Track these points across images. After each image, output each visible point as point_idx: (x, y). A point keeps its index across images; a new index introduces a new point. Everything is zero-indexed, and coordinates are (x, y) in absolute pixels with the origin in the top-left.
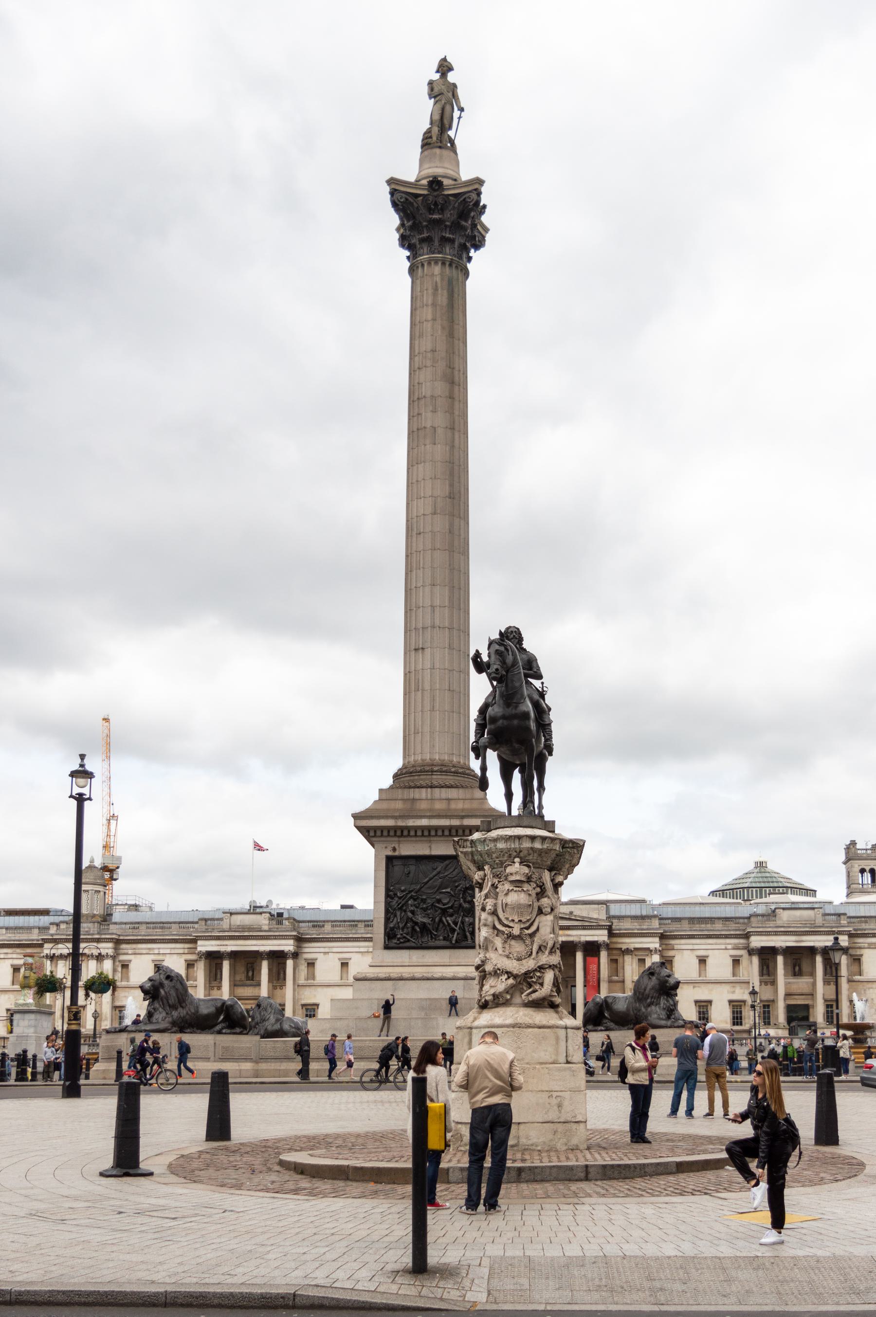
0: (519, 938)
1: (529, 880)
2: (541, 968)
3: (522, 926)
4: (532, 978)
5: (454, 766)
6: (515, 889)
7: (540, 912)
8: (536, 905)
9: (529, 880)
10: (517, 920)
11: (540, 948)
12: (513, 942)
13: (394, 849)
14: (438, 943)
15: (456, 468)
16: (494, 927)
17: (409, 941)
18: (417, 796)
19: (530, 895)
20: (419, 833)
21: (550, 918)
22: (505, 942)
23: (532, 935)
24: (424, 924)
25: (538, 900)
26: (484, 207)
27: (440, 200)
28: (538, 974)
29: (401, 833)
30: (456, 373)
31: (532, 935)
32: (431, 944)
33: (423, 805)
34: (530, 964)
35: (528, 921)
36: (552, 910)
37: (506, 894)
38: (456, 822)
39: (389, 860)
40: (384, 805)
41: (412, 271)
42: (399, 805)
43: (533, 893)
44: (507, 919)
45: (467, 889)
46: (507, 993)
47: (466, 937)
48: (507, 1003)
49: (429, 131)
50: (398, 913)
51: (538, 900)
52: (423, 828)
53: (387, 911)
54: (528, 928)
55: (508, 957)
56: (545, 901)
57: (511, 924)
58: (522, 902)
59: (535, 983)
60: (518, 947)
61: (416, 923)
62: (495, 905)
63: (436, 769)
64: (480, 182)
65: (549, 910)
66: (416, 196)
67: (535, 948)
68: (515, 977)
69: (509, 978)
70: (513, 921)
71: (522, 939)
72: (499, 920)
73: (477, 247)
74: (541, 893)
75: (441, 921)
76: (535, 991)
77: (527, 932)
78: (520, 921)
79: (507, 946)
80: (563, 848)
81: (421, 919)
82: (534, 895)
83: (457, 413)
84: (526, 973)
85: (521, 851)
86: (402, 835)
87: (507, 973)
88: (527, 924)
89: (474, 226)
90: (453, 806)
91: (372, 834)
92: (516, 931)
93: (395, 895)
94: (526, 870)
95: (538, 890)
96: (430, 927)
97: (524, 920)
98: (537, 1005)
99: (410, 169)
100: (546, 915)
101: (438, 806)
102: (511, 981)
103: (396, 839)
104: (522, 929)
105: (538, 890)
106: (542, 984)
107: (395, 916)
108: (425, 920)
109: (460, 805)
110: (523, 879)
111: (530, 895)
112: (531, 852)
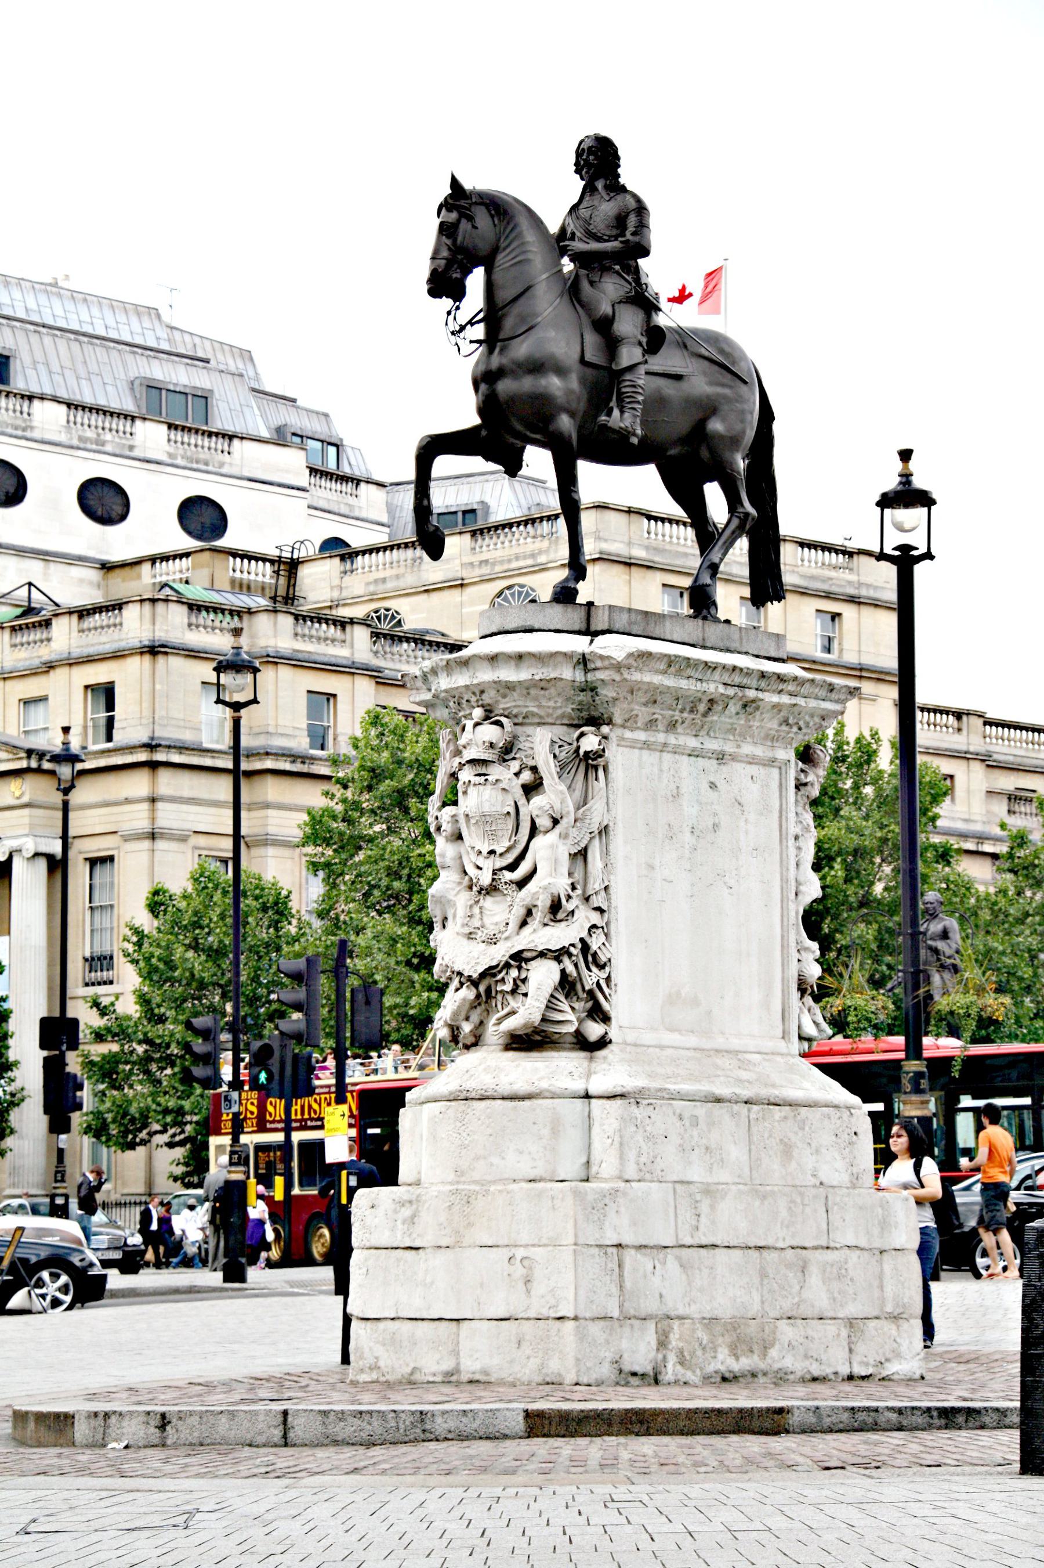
0: (492, 890)
1: (506, 752)
9: (506, 752)
10: (485, 852)
11: (529, 913)
12: (488, 902)
21: (553, 837)
31: (521, 884)
34: (499, 954)
35: (509, 850)
36: (556, 822)
37: (465, 793)
46: (467, 1019)
48: (476, 1041)
54: (512, 867)
55: (470, 936)
56: (538, 801)
58: (486, 808)
60: (499, 912)
62: (454, 818)
65: (548, 823)
67: (519, 912)
68: (475, 983)
69: (462, 984)
76: (513, 1013)
77: (508, 876)
79: (476, 910)
80: (586, 671)
84: (489, 973)
85: (482, 692)
88: (510, 859)
97: (499, 850)
98: (528, 1041)
102: (468, 993)
105: (527, 776)
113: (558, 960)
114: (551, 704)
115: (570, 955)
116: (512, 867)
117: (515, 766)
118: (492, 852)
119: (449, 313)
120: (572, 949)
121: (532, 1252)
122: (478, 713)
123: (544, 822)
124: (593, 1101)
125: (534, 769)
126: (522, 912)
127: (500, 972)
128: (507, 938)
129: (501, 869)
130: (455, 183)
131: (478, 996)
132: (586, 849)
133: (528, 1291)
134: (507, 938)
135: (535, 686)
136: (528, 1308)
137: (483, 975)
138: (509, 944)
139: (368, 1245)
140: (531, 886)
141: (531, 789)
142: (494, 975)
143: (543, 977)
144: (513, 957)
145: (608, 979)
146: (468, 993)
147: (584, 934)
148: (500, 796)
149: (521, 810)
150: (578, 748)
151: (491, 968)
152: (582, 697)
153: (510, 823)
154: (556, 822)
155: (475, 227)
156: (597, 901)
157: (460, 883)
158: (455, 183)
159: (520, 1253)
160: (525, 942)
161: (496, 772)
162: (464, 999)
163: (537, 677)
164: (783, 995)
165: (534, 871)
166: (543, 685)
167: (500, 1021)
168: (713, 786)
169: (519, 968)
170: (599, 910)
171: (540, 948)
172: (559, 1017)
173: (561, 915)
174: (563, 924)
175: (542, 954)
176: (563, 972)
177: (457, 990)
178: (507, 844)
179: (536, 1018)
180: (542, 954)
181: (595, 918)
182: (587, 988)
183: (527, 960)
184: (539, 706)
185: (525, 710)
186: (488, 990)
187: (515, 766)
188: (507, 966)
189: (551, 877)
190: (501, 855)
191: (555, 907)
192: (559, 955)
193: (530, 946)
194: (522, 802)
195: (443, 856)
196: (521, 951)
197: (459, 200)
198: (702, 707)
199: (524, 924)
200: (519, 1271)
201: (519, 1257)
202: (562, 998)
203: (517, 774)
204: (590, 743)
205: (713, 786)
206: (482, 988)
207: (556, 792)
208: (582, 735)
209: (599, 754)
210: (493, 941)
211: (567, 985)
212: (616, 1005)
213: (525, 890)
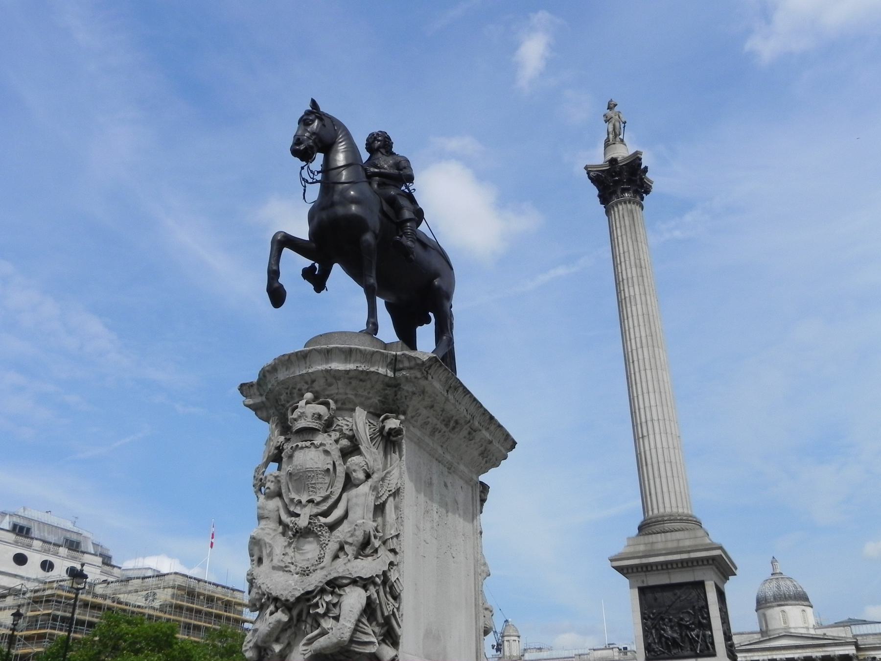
1: (328, 426)
2: (334, 585)
3: (315, 510)
4: (316, 605)
5: (679, 515)
6: (300, 444)
7: (349, 483)
8: (341, 470)
10: (304, 501)
11: (342, 548)
13: (643, 582)
14: (686, 653)
15: (651, 318)
16: (280, 522)
17: (664, 653)
18: (655, 540)
19: (326, 452)
20: (659, 568)
21: (364, 488)
22: (290, 544)
23: (332, 527)
24: (674, 639)
25: (345, 463)
26: (646, 168)
28: (328, 598)
29: (646, 568)
30: (642, 262)
31: (332, 527)
32: (681, 654)
33: (660, 546)
34: (316, 580)
35: (325, 499)
36: (368, 476)
37: (291, 457)
38: (685, 556)
39: (643, 591)
40: (631, 549)
41: (608, 213)
42: (642, 548)
44: (292, 500)
45: (703, 607)
46: (277, 640)
47: (708, 648)
49: (608, 138)
50: (653, 631)
51: (345, 463)
52: (662, 564)
53: (644, 630)
54: (325, 514)
56: (355, 460)
57: (298, 510)
59: (325, 615)
61: (667, 639)
63: (666, 518)
67: (333, 546)
69: (277, 609)
70: (300, 502)
71: (317, 536)
73: (647, 192)
74: (352, 449)
75: (687, 635)
76: (324, 633)
80: (395, 370)
81: (669, 633)
82: (336, 454)
83: (646, 284)
85: (313, 381)
86: (647, 571)
87: (276, 600)
88: (324, 507)
89: (642, 179)
90: (681, 544)
91: (625, 571)
92: (303, 522)
93: (649, 617)
94: (321, 409)
95: (345, 442)
96: (679, 641)
97: (318, 499)
99: (599, 158)
101: (670, 545)
102: (282, 616)
103: (643, 574)
104: (311, 517)
105: (345, 442)
106: (337, 618)
107: (652, 633)
108: (675, 635)
109: (687, 543)
110: (312, 425)
111: (326, 452)
112: (330, 380)
113: (365, 588)
114: (365, 393)
115: (375, 584)
116: (325, 514)
117: (335, 435)
118: (311, 501)
119: (302, 168)
120: (377, 579)
122: (309, 395)
125: (353, 438)
126: (337, 546)
127: (315, 597)
128: (322, 568)
129: (316, 515)
130: (314, 103)
131: (291, 619)
132: (383, 504)
134: (322, 568)
135: (356, 378)
137: (298, 599)
138: (324, 572)
140: (345, 527)
141: (345, 454)
142: (309, 600)
143: (353, 600)
144: (329, 583)
145: (398, 609)
146: (282, 616)
147: (386, 568)
148: (322, 456)
149: (338, 468)
150: (384, 427)
151: (308, 593)
152: (389, 392)
153: (327, 480)
154: (368, 476)
155: (324, 125)
156: (392, 544)
157: (275, 530)
158: (314, 103)
160: (340, 570)
161: (319, 439)
162: (279, 622)
163: (360, 369)
164: (476, 640)
165: (346, 516)
166: (362, 377)
167: (310, 642)
168: (446, 485)
169: (332, 593)
170: (393, 551)
171: (355, 575)
172: (365, 638)
173: (368, 551)
174: (370, 558)
175: (354, 582)
176: (369, 598)
177: (272, 613)
178: (324, 494)
179: (347, 636)
180: (354, 582)
181: (391, 557)
182: (386, 614)
183: (341, 587)
184: (356, 395)
185: (344, 397)
186: (300, 615)
187: (335, 435)
188: (322, 591)
189: (361, 519)
190: (318, 504)
191: (366, 543)
192: (364, 583)
193: (346, 574)
194: (339, 462)
196: (336, 579)
197: (314, 111)
198: (452, 424)
199: (336, 557)
202: (366, 623)
203: (337, 441)
204: (393, 423)
205: (446, 485)
206: (295, 613)
207: (371, 455)
208: (386, 418)
209: (397, 432)
210: (305, 573)
211: (369, 610)
212: (407, 631)
213: (336, 533)
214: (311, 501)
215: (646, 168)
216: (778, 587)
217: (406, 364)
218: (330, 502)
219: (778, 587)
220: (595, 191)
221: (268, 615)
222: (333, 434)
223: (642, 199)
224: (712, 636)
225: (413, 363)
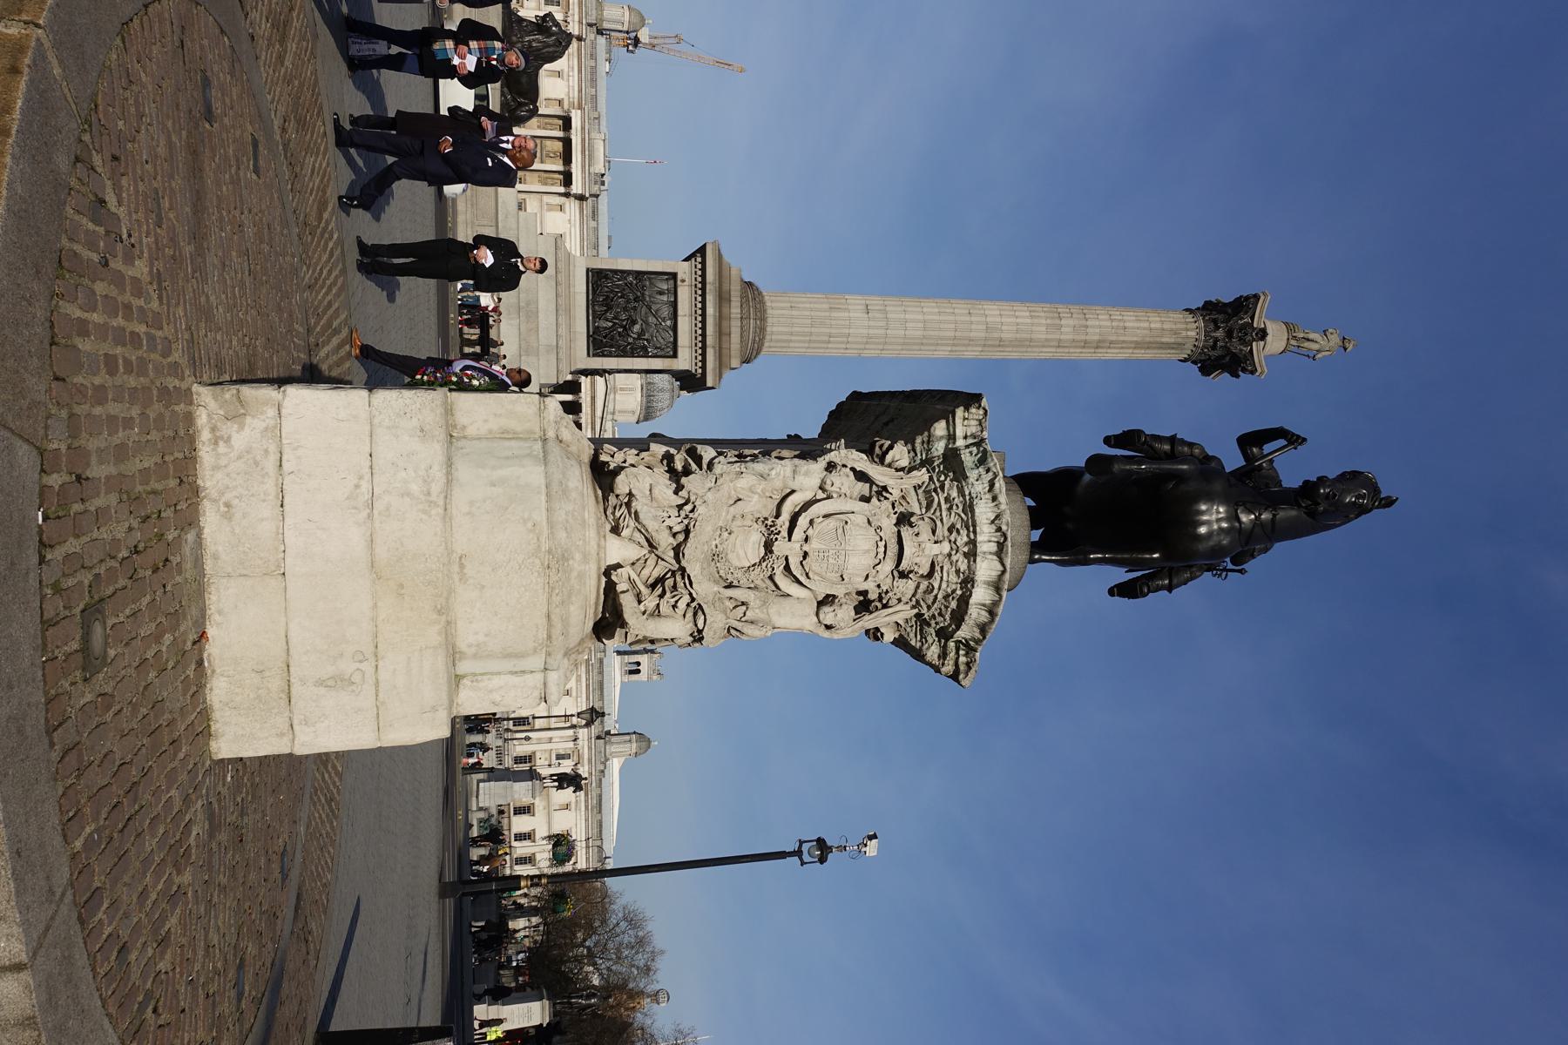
12: (756, 538)
26: (1238, 376)
27: (1249, 338)
36: (828, 627)
43: (870, 586)
57: (798, 534)
64: (1253, 372)
66: (1252, 318)
68: (678, 551)
72: (807, 506)
73: (1201, 369)
77: (779, 571)
78: (806, 555)
80: (958, 642)
82: (863, 587)
87: (687, 532)
92: (781, 547)
100: (817, 615)
116: (787, 568)
121: (369, 689)
123: (828, 615)
124: (540, 676)
130: (1389, 502)
133: (320, 683)
136: (303, 682)
139: (376, 421)
158: (1389, 502)
159: (368, 667)
161: (888, 566)
195: (807, 474)
200: (347, 667)
201: (363, 666)
214: (806, 555)
215: (1238, 376)
216: (662, 390)
217: (962, 659)
218: (803, 579)
219: (662, 390)
220: (1227, 298)
221: (668, 522)
222: (889, 580)
223: (1195, 362)
224: (610, 356)
225: (962, 668)
